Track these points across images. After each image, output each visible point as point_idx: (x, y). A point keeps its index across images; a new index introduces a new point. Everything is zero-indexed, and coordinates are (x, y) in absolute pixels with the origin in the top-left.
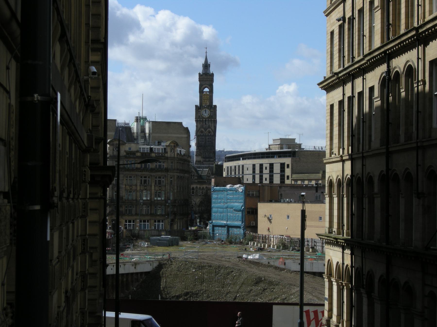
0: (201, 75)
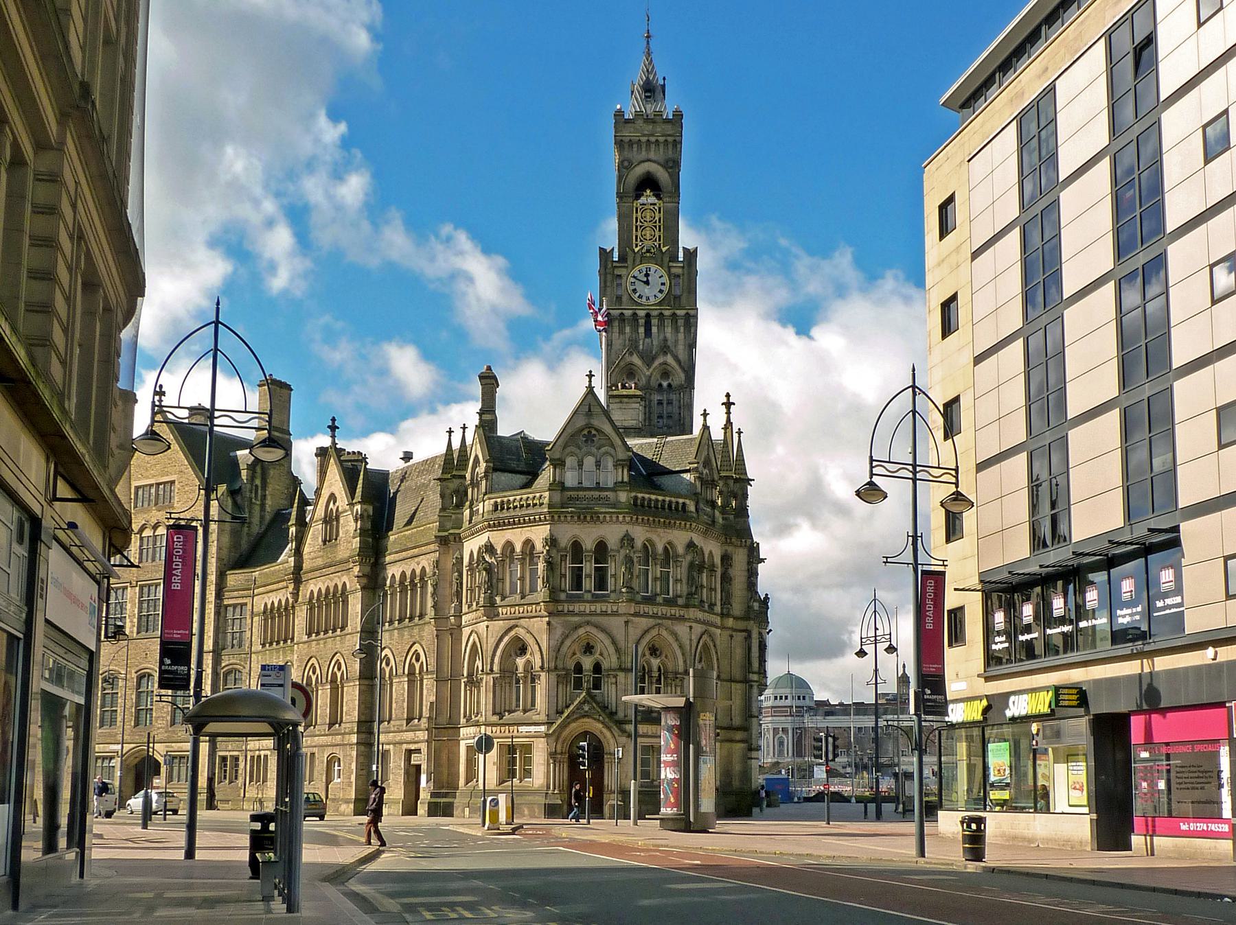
0: (628, 121)
